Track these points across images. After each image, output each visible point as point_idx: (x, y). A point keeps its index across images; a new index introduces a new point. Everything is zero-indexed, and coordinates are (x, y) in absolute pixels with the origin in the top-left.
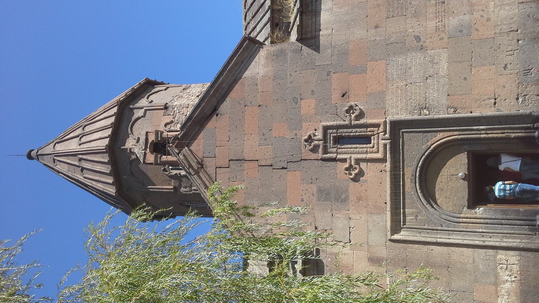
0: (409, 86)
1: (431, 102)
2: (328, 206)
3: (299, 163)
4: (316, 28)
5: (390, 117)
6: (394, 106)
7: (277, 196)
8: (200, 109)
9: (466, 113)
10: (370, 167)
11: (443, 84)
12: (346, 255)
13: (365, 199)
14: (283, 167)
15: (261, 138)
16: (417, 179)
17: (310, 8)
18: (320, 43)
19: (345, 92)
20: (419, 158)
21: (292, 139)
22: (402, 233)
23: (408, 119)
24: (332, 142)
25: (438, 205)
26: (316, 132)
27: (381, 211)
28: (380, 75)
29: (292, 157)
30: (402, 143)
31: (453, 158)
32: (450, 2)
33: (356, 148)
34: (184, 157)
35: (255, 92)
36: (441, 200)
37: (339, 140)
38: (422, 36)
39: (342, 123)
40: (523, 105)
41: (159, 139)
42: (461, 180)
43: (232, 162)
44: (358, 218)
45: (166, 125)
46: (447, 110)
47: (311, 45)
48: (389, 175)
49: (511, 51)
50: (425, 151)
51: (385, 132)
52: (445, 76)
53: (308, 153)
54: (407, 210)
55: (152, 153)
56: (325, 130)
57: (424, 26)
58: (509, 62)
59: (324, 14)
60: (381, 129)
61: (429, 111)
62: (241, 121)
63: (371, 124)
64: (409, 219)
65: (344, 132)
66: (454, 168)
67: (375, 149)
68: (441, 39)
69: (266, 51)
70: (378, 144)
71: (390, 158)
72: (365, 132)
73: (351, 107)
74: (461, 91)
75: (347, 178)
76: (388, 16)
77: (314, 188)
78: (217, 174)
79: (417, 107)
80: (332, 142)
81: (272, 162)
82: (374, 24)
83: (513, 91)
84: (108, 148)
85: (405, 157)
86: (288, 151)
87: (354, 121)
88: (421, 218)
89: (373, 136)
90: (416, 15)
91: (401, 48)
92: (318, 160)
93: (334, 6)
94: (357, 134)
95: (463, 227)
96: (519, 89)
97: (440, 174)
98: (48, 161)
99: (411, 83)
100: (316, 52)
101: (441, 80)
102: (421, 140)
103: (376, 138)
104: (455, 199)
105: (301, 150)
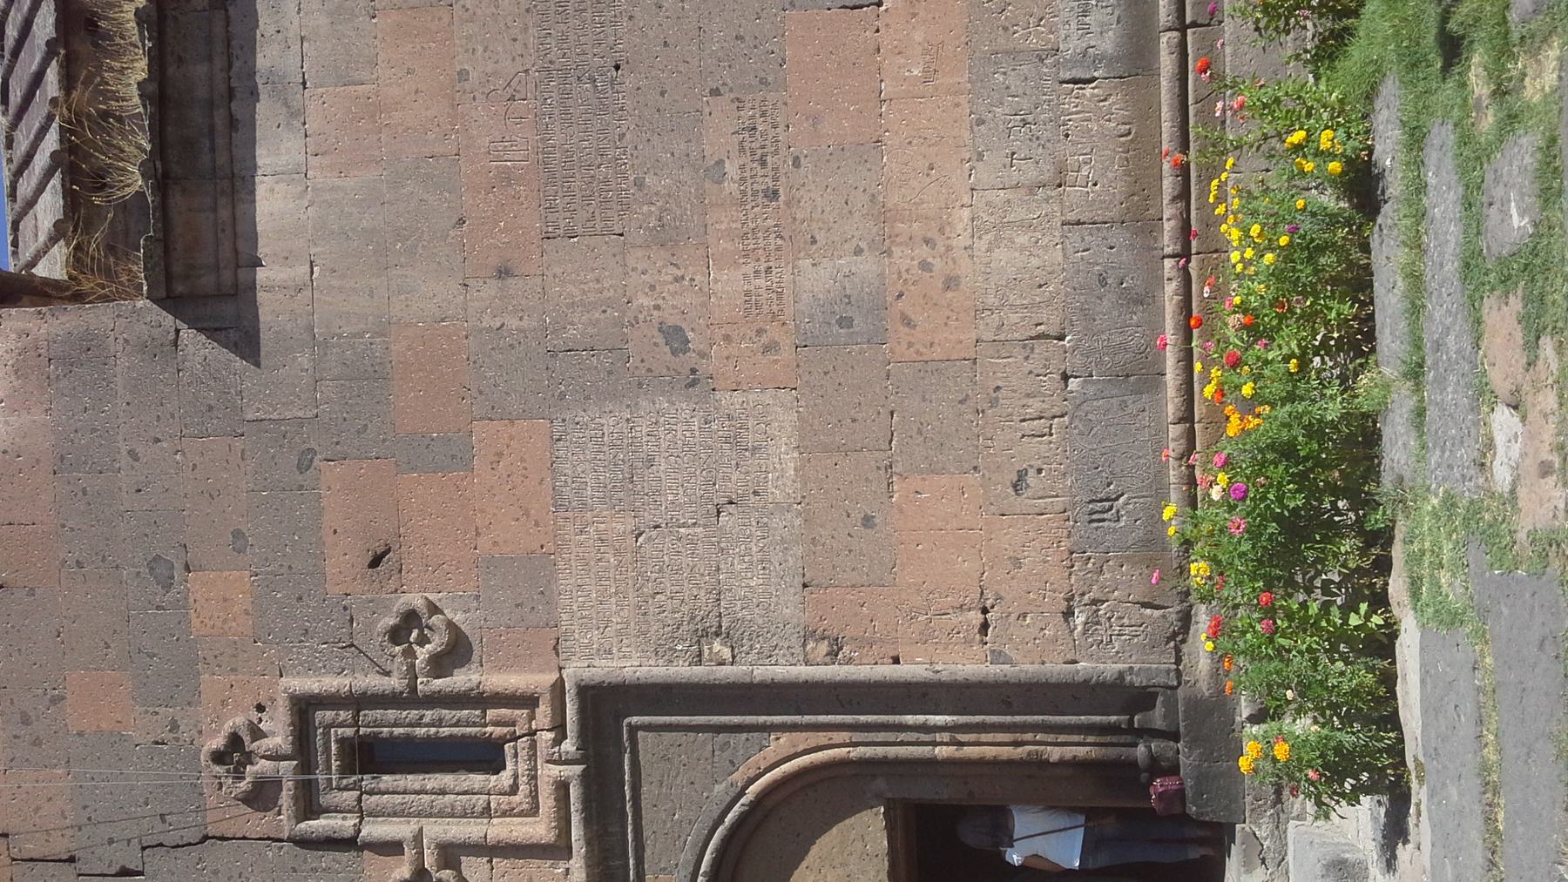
1: (738, 608)
3: (195, 852)
4: (236, 252)
5: (579, 664)
6: (591, 619)
9: (876, 663)
11: (783, 540)
15: (16, 737)
17: (206, 159)
18: (262, 319)
19: (382, 549)
20: (702, 837)
23: (651, 681)
26: (264, 719)
28: (527, 482)
29: (160, 827)
30: (632, 775)
31: (834, 830)
32: (798, 196)
33: (443, 792)
38: (693, 330)
39: (373, 682)
40: (1090, 640)
46: (804, 645)
47: (217, 325)
49: (1041, 418)
51: (559, 729)
52: (790, 505)
53: (234, 811)
57: (700, 289)
58: (1032, 463)
59: (272, 190)
60: (544, 713)
61: (733, 648)
63: (497, 693)
65: (391, 724)
66: (840, 871)
68: (767, 349)
69: (14, 336)
70: (534, 777)
71: (582, 842)
72: (474, 725)
76: (550, 229)
79: (685, 627)
80: (335, 764)
81: (72, 846)
83: (1052, 584)
86: (142, 800)
89: (512, 744)
90: (665, 237)
91: (610, 373)
92: (281, 840)
93: (313, 161)
94: (445, 731)
96: (1073, 577)
99: (656, 527)
100: (242, 358)
101: (776, 522)
102: (707, 759)
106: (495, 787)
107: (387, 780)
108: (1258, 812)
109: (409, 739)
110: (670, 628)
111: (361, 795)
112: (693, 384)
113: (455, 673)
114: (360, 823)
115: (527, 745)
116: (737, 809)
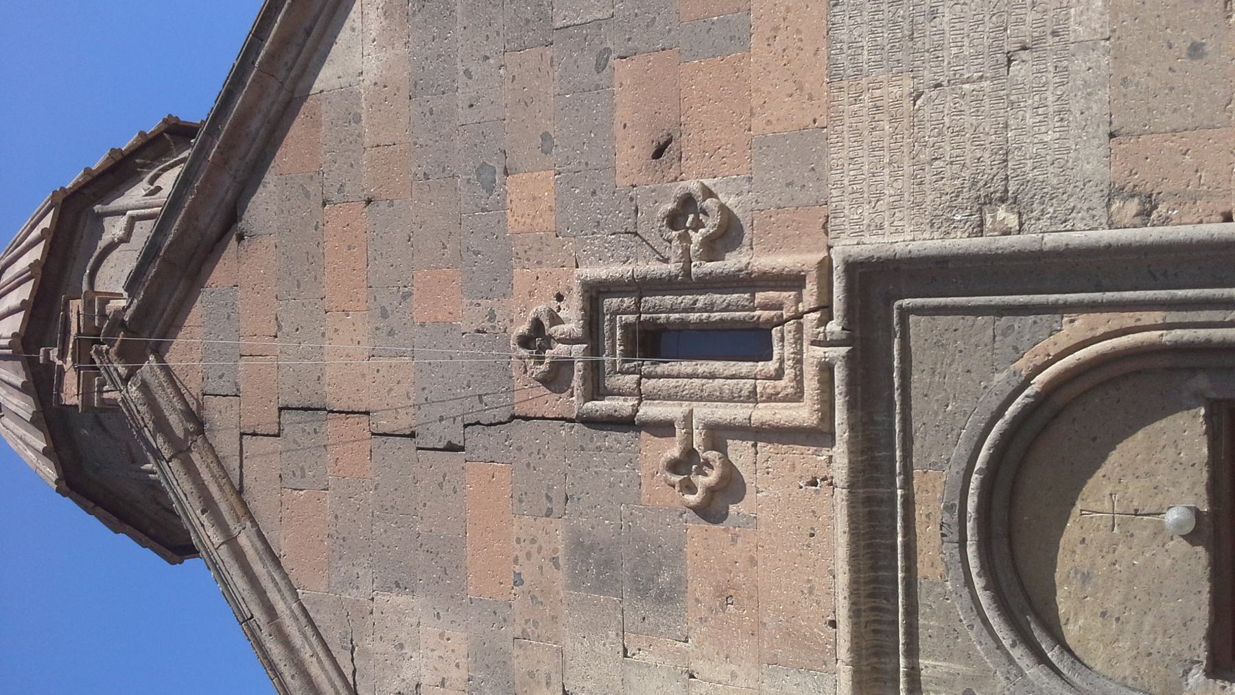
1: (1028, 169)
2: (609, 615)
5: (848, 242)
7: (433, 556)
8: (181, 217)
9: (1201, 222)
10: (768, 461)
13: (750, 598)
14: (449, 442)
15: (377, 329)
16: (969, 525)
19: (665, 139)
20: (978, 431)
21: (478, 331)
23: (923, 253)
24: (619, 349)
25: (1066, 648)
28: (802, 53)
29: (479, 407)
31: (1140, 435)
33: (712, 376)
34: (144, 393)
35: (351, 146)
36: (1081, 622)
39: (655, 268)
41: (96, 324)
42: (1177, 539)
43: (287, 416)
44: (720, 678)
46: (1108, 205)
48: (845, 503)
50: (1005, 395)
51: (825, 309)
52: (1096, 42)
53: (536, 392)
54: (926, 662)
56: (591, 297)
60: (810, 295)
61: (1020, 215)
62: (311, 260)
63: (765, 273)
67: (785, 384)
70: (799, 362)
71: (845, 426)
72: (744, 309)
73: (687, 202)
74: (1175, 111)
75: (677, 504)
77: (557, 535)
78: (244, 456)
80: (619, 349)
81: (413, 423)
84: (19, 341)
85: (916, 424)
86: (465, 383)
87: (700, 259)
89: (779, 328)
92: (571, 421)
94: (716, 316)
97: (1079, 505)
99: (936, 86)
101: (1078, 65)
102: (986, 345)
103: (791, 335)
104: (1147, 627)
105: (511, 377)
106: (761, 371)
107: (662, 368)
109: (683, 322)
110: (948, 197)
111: (641, 378)
113: (727, 257)
114: (639, 404)
115: (793, 328)
116: (1020, 401)
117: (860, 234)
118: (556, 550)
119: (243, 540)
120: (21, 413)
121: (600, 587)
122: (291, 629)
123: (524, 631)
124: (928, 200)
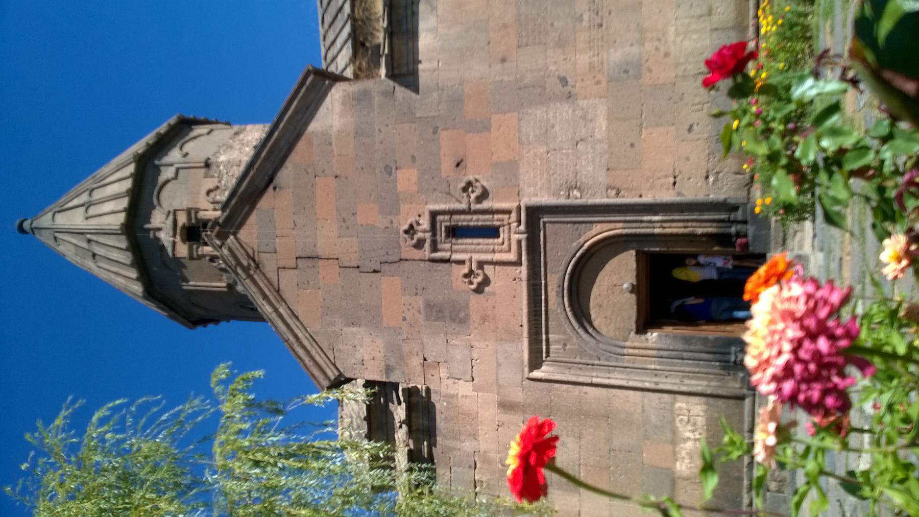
0: (552, 155)
3: (397, 265)
4: (414, 59)
11: (600, 153)
12: (468, 399)
13: (493, 319)
15: (341, 226)
22: (544, 368)
25: (594, 329)
27: (514, 337)
33: (479, 244)
36: (599, 320)
37: (455, 232)
45: (209, 192)
46: (607, 191)
51: (519, 221)
55: (184, 241)
60: (514, 216)
64: (555, 349)
65: (462, 220)
67: (505, 246)
68: (598, 83)
70: (510, 239)
72: (489, 221)
73: (469, 184)
77: (420, 302)
80: (443, 235)
82: (500, 56)
85: (548, 259)
88: (572, 347)
90: (561, 44)
92: (425, 261)
94: (480, 223)
95: (629, 361)
98: (46, 238)
107: (460, 241)
108: (776, 248)
109: (468, 227)
112: (570, 97)
117: (530, 197)
118: (420, 307)
119: (281, 310)
120: (121, 260)
121: (438, 319)
122: (306, 343)
123: (407, 337)
124: (553, 186)
